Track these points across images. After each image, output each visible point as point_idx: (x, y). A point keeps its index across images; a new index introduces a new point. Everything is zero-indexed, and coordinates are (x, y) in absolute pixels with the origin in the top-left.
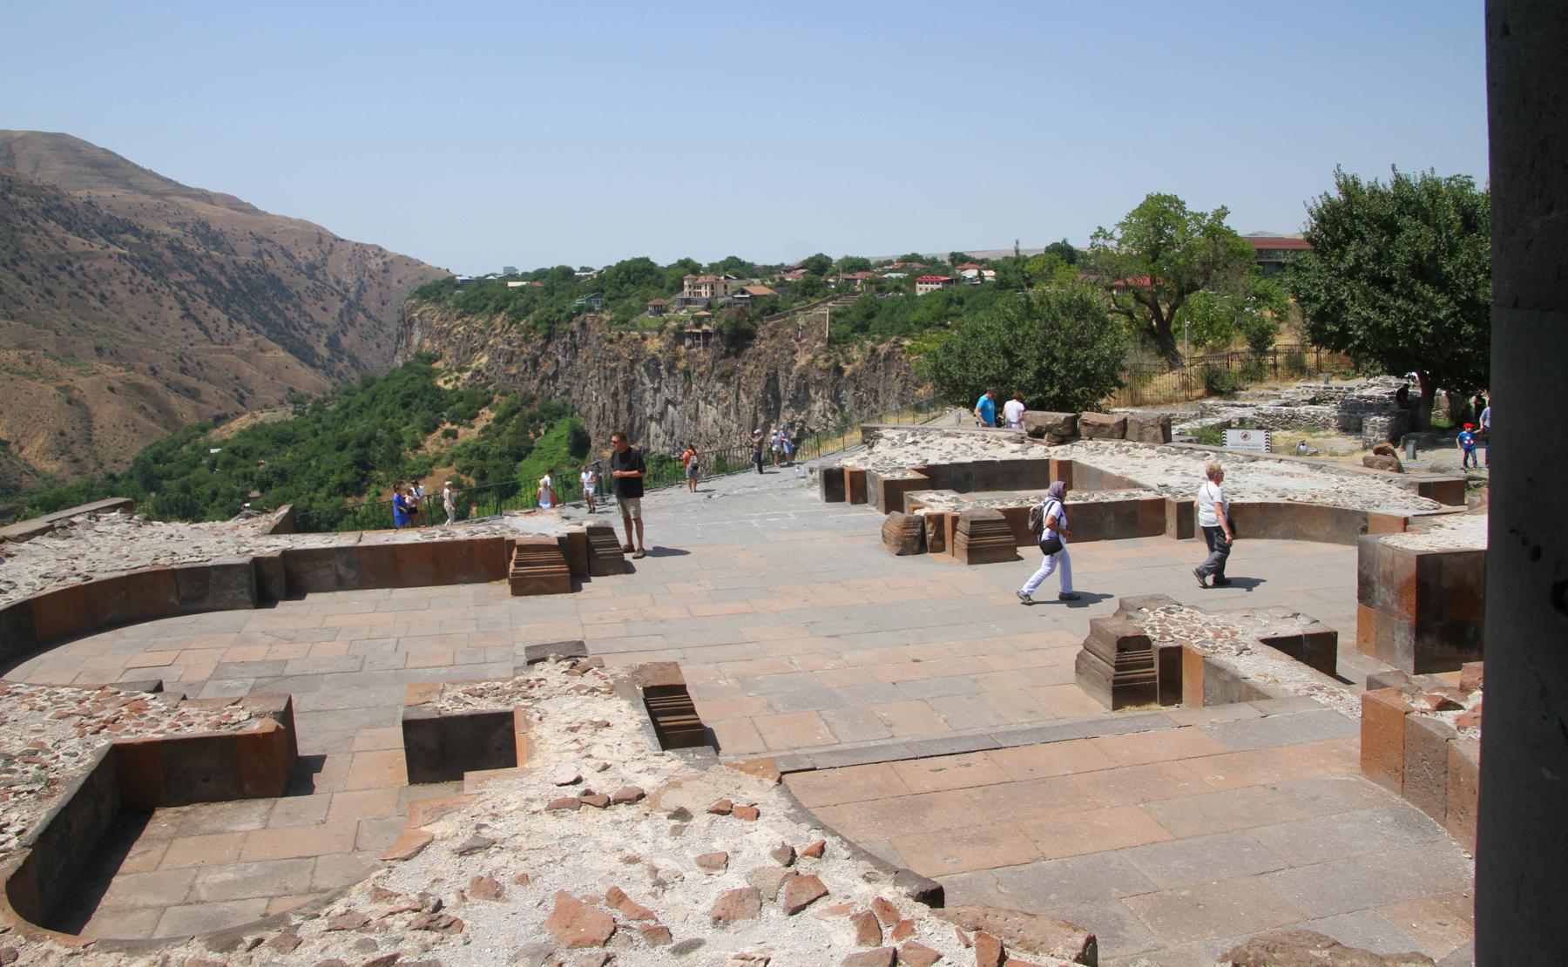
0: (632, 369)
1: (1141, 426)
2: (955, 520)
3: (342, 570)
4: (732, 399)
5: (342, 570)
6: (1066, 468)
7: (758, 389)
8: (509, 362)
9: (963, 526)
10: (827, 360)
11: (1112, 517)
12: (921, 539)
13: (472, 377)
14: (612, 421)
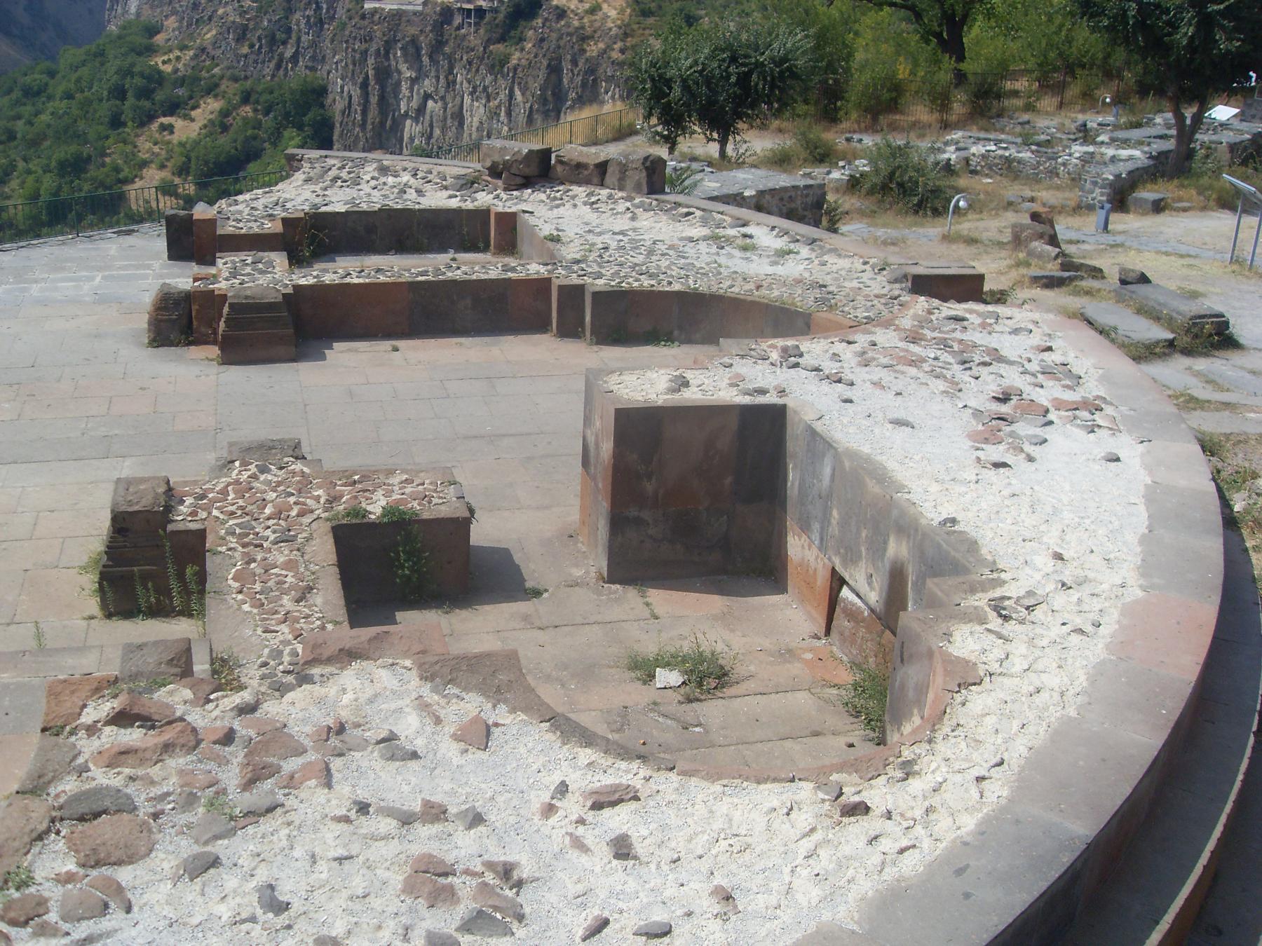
0: (387, 53)
1: (624, 169)
2: (224, 297)
4: (503, 96)
6: (509, 222)
7: (535, 86)
8: (240, 39)
10: (622, 51)
11: (469, 301)
12: (178, 323)
13: (196, 56)
14: (359, 117)
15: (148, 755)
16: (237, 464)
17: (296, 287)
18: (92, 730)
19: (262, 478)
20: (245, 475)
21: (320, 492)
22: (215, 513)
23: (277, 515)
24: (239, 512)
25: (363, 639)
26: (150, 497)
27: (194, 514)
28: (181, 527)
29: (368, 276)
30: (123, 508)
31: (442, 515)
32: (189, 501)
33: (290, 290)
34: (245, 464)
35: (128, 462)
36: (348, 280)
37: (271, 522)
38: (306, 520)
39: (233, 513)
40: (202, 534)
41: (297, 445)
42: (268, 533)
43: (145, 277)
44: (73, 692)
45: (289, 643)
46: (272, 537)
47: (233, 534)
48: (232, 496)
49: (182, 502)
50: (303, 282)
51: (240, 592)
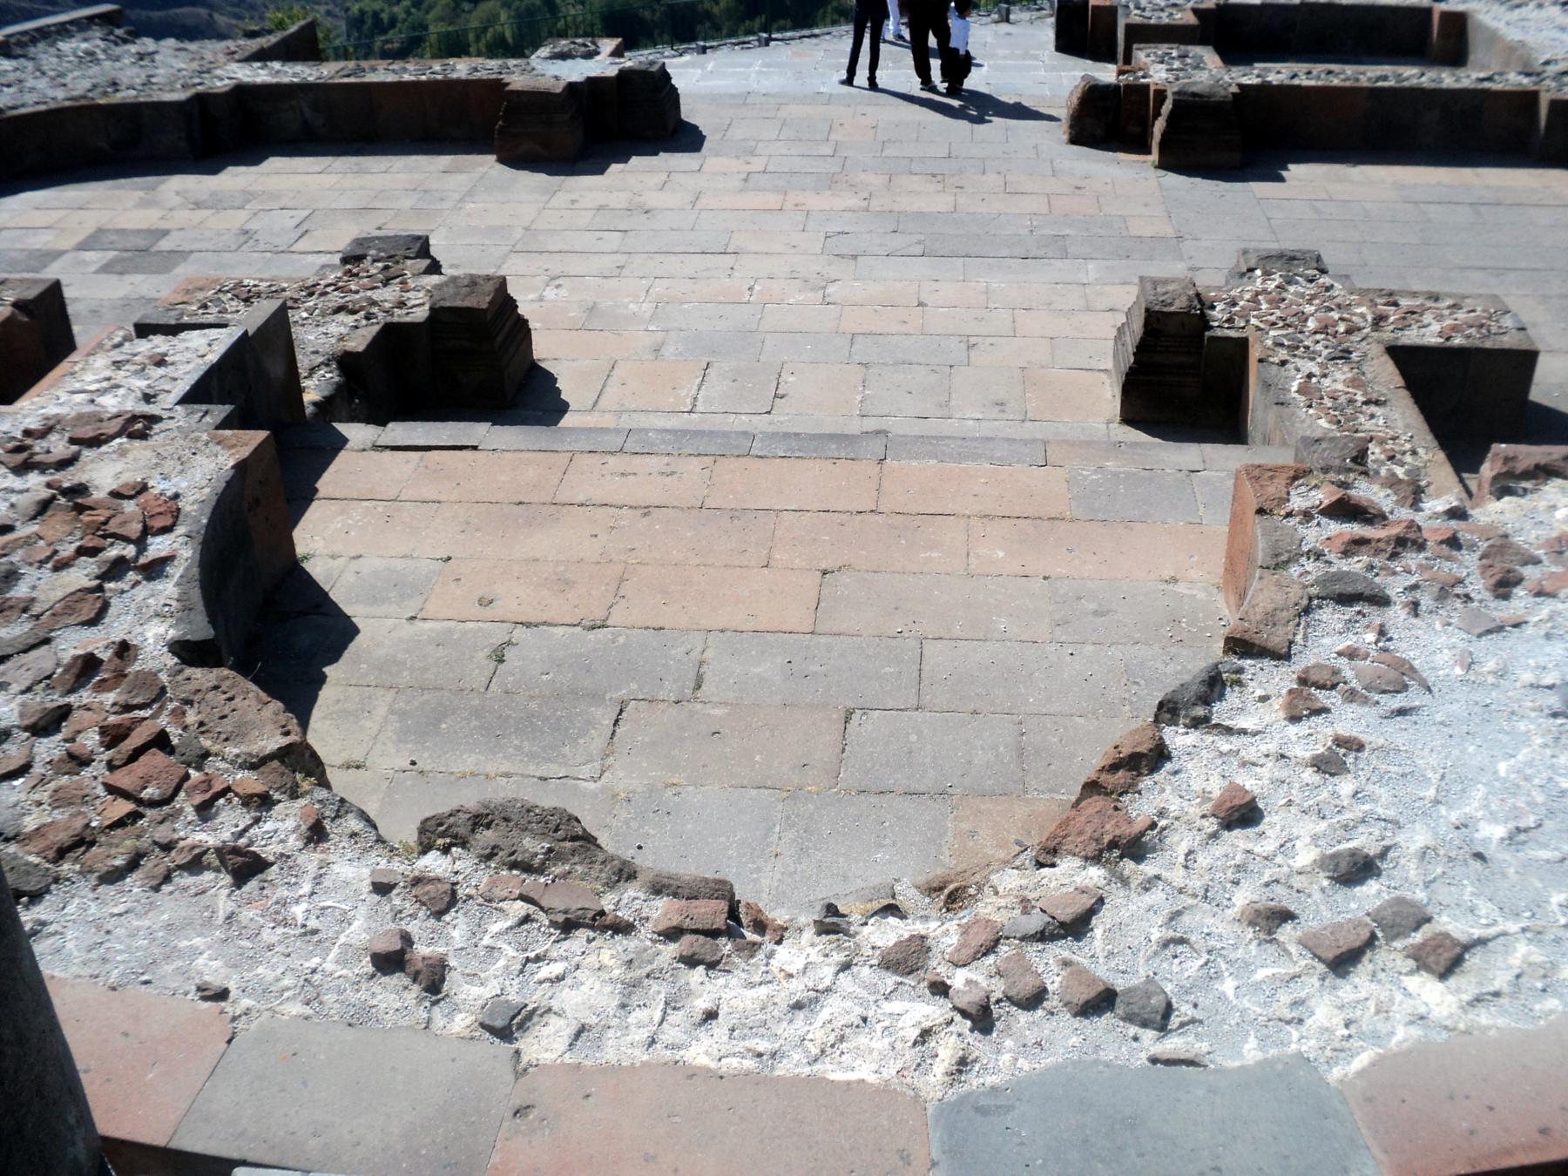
2: (1161, 95)
3: (308, 113)
5: (308, 113)
9: (1167, 107)
12: (1106, 121)
15: (1382, 545)
16: (1258, 272)
17: (1240, 86)
18: (1307, 515)
19: (1292, 289)
20: (1271, 285)
21: (1362, 309)
22: (1253, 321)
23: (1323, 329)
24: (1281, 324)
25: (1555, 457)
26: (1184, 298)
27: (1229, 320)
28: (1219, 333)
29: (1318, 78)
30: (1157, 308)
31: (1507, 346)
32: (1220, 306)
33: (1234, 89)
34: (1267, 274)
35: (1091, 266)
36: (1296, 82)
37: (1319, 337)
38: (1355, 337)
39: (1274, 324)
40: (1243, 344)
41: (1319, 259)
42: (1319, 347)
43: (1036, 68)
44: (1271, 478)
45: (1383, 463)
46: (1325, 352)
47: (1282, 345)
48: (1264, 306)
49: (1213, 308)
50: (1246, 81)
51: (1310, 406)
